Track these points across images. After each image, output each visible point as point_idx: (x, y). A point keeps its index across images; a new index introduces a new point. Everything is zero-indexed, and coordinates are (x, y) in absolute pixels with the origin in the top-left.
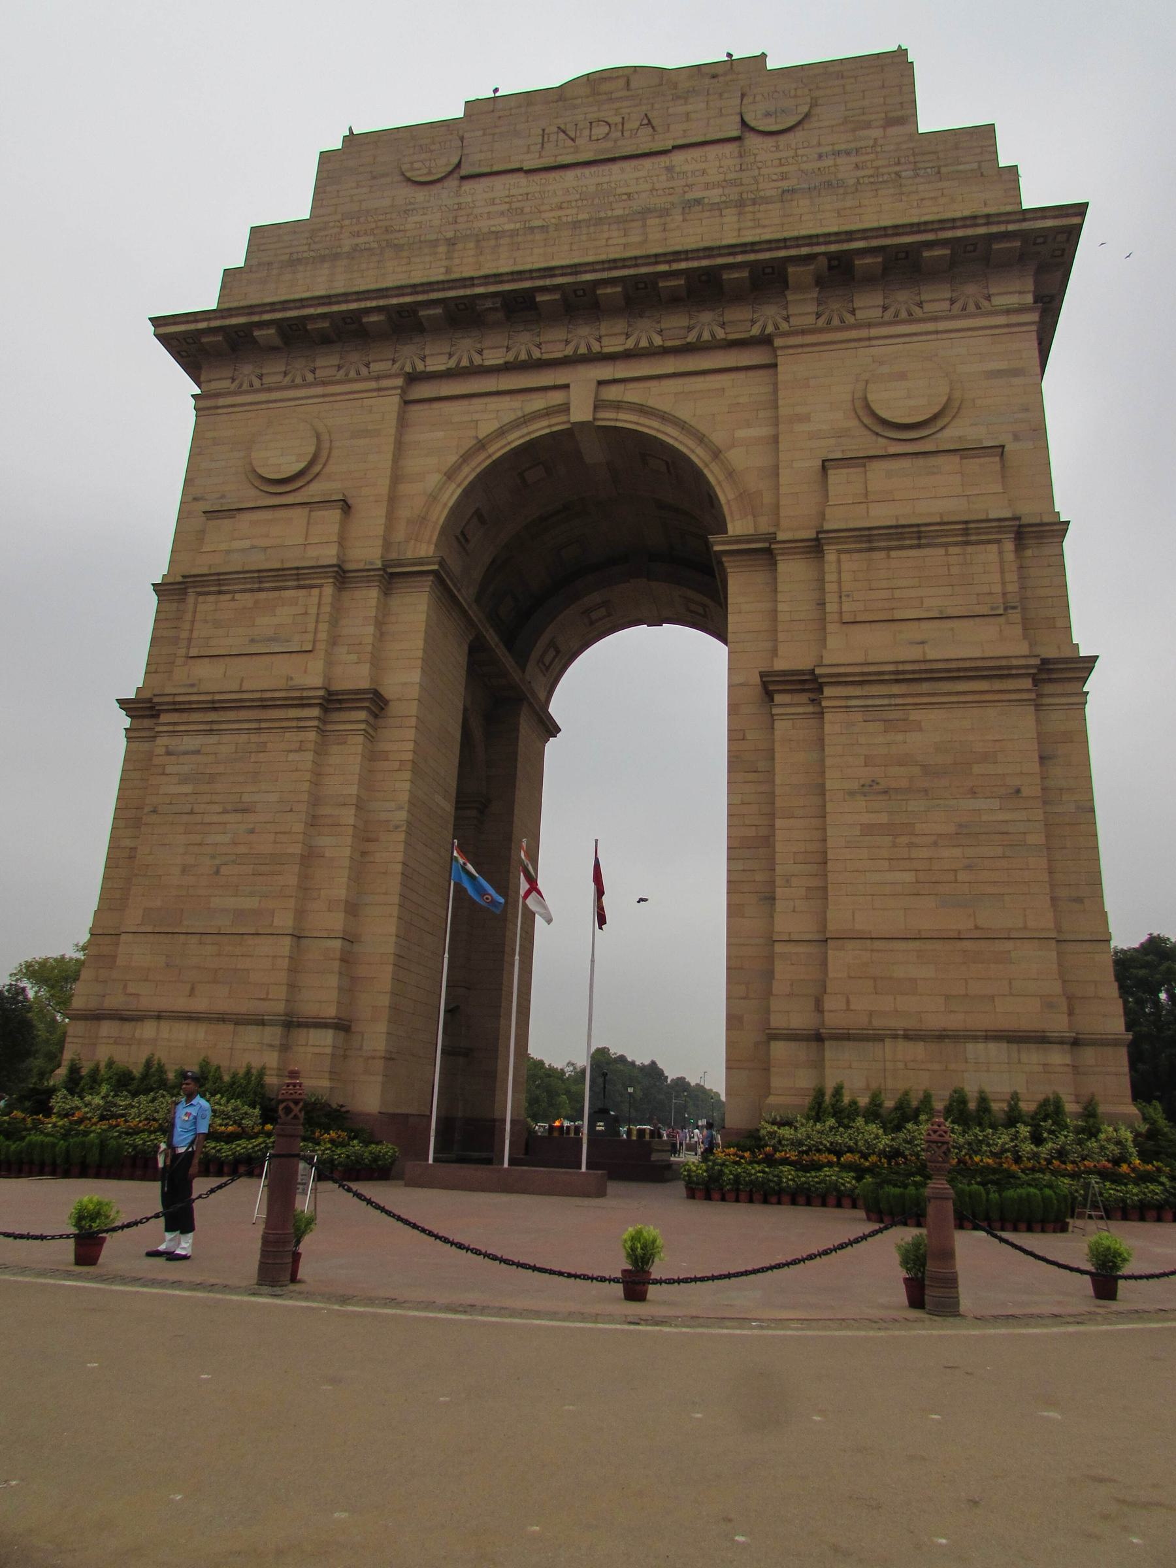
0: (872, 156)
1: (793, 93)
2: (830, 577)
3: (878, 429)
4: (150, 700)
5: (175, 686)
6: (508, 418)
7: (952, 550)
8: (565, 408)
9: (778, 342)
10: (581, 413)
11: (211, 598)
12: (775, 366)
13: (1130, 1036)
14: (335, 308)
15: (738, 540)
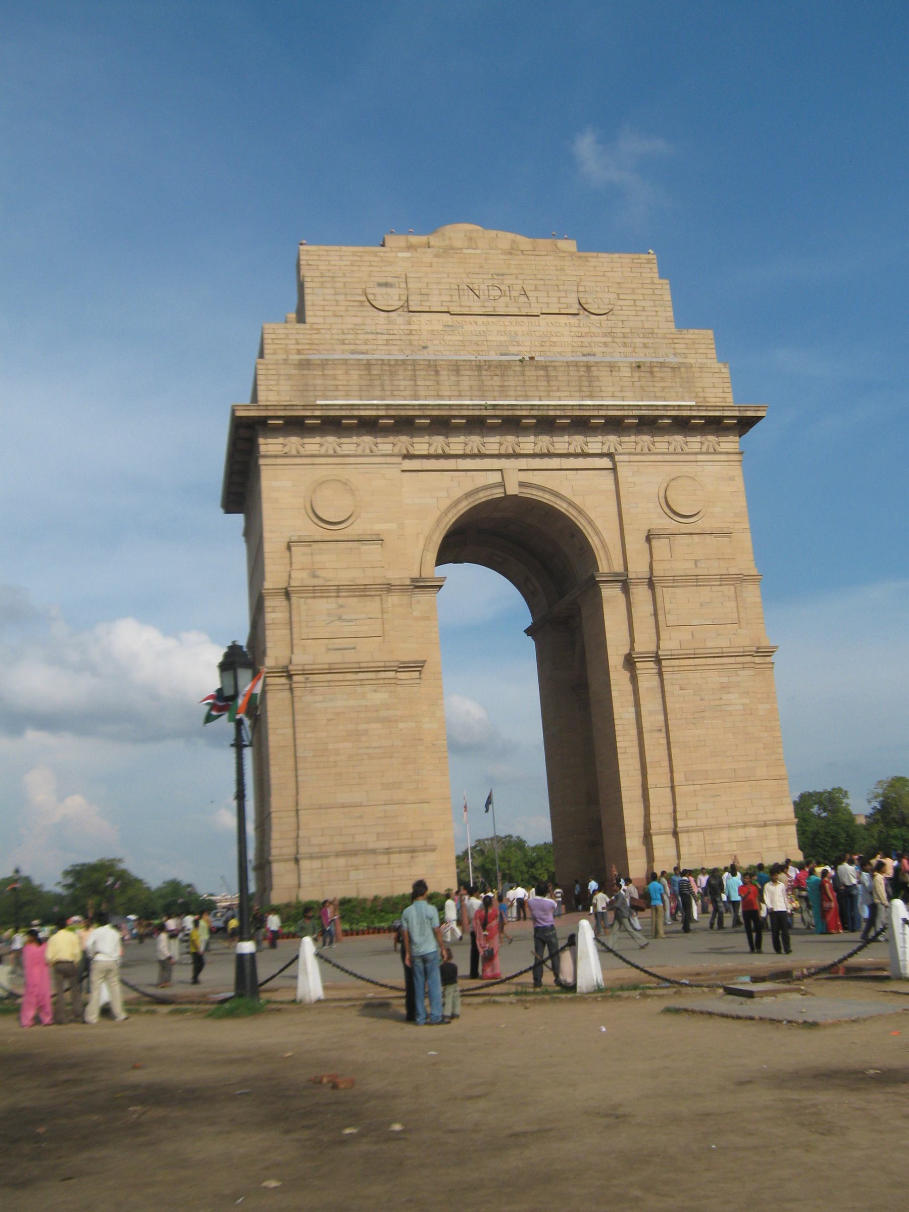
0: (652, 341)
1: (606, 289)
2: (659, 600)
3: (671, 515)
4: (287, 667)
5: (300, 659)
6: (469, 487)
7: (714, 588)
8: (502, 485)
9: (617, 458)
10: (513, 489)
11: (309, 601)
12: (614, 469)
13: (796, 820)
14: (363, 413)
15: (607, 575)
